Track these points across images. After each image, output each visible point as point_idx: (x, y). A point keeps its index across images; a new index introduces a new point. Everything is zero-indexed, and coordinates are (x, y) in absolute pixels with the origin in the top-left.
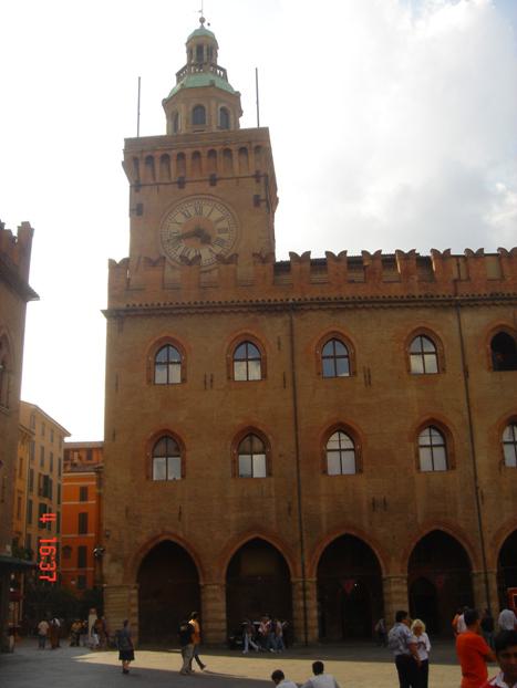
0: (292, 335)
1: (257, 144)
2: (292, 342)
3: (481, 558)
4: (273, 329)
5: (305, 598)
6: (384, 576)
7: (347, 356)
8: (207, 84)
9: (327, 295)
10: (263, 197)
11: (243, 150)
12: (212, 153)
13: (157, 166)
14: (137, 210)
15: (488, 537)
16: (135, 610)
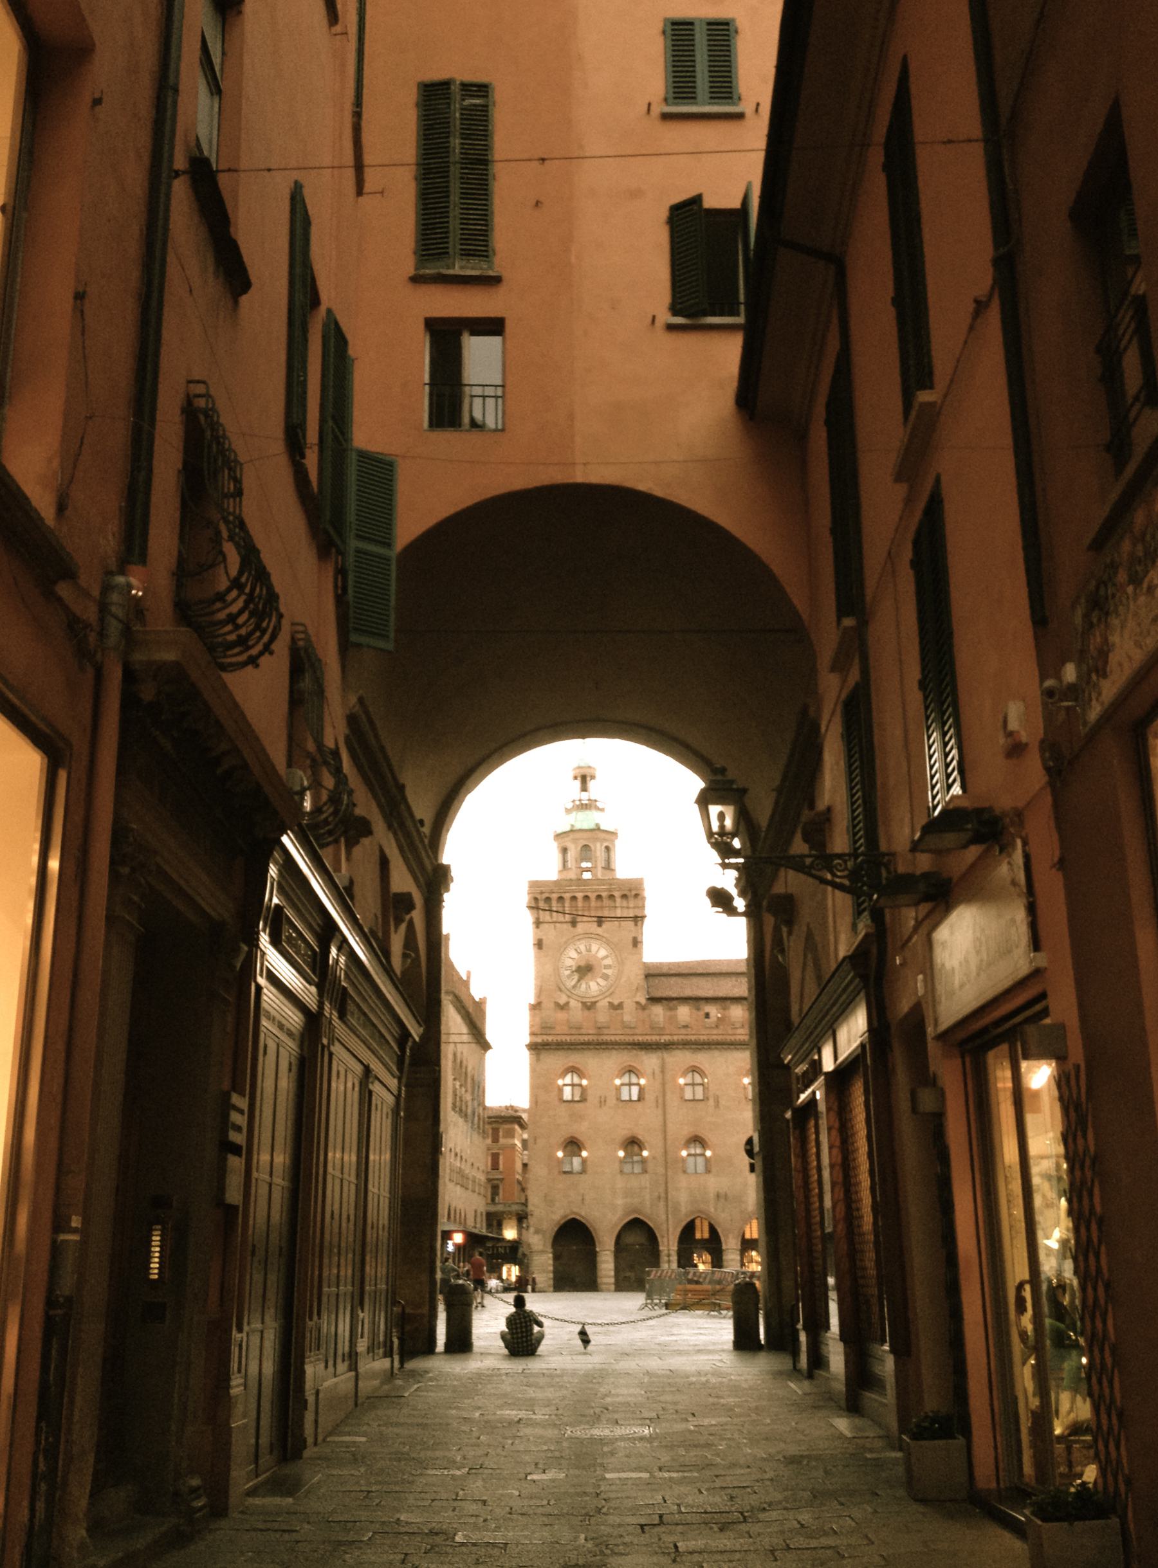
1: (632, 892)
2: (663, 1072)
4: (650, 1061)
5: (669, 1262)
6: (724, 1247)
7: (702, 1084)
8: (592, 826)
9: (689, 1038)
11: (624, 896)
12: (599, 897)
14: (539, 944)
16: (551, 1268)
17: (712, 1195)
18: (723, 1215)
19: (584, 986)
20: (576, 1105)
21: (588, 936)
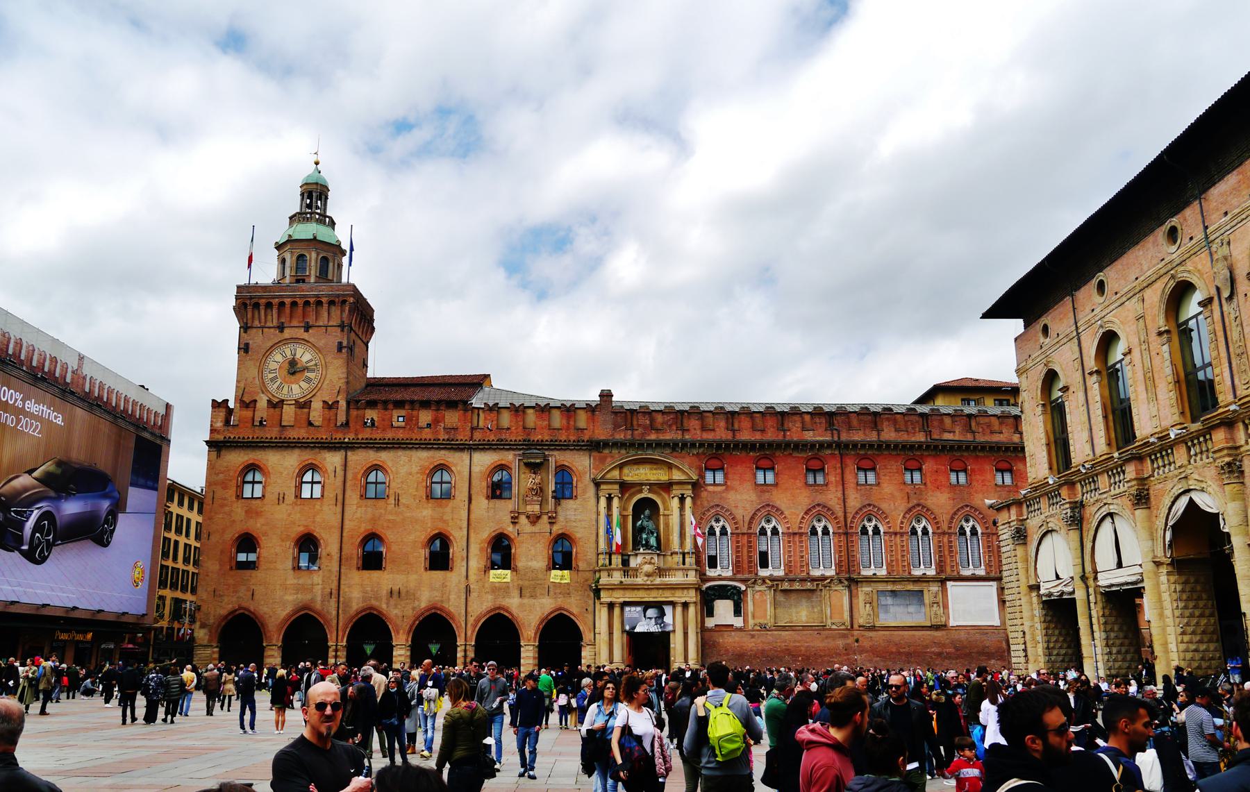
0: (345, 465)
3: (463, 635)
4: (333, 460)
9: (374, 436)
10: (345, 344)
12: (307, 303)
13: (262, 312)
14: (244, 348)
15: (471, 620)
17: (384, 592)
18: (395, 611)
19: (286, 389)
20: (253, 502)
21: (296, 340)
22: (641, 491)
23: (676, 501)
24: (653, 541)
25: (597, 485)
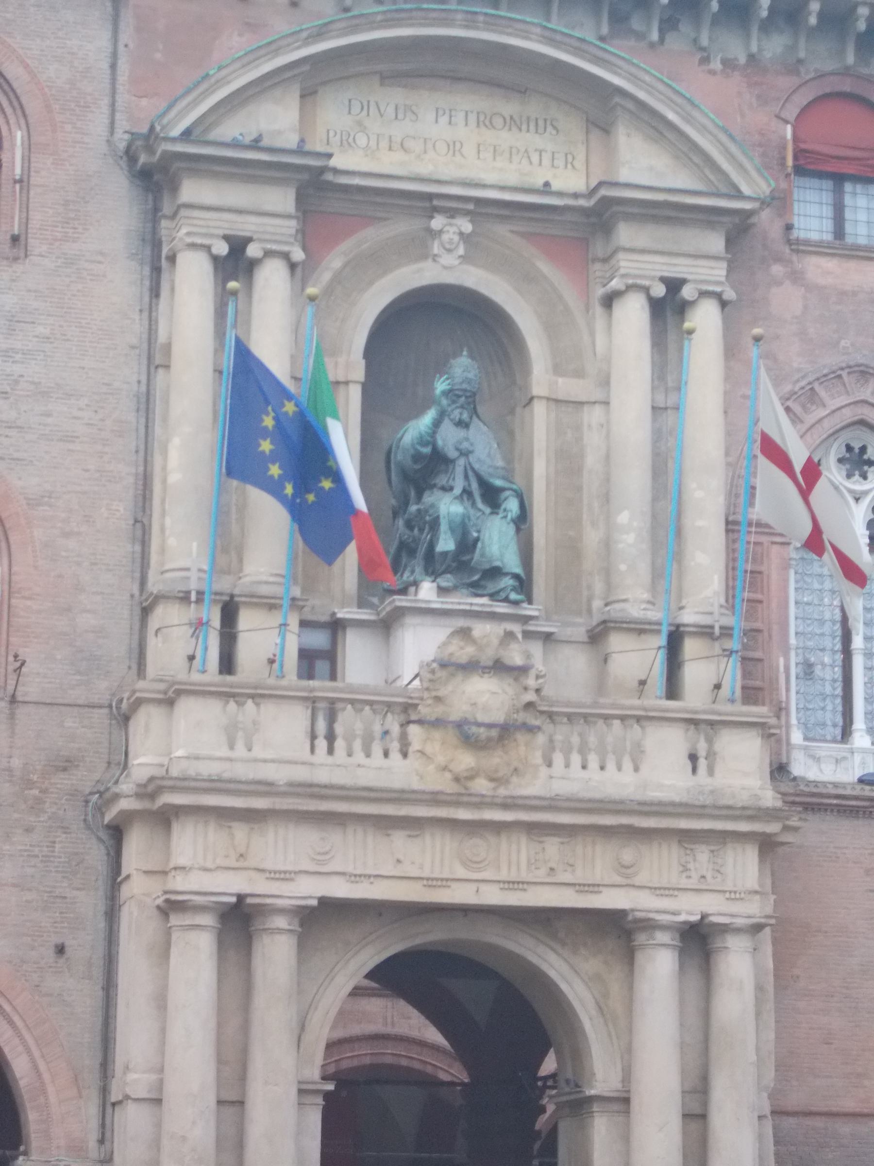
22: (419, 247)
23: (633, 313)
24: (497, 541)
25: (154, 175)
